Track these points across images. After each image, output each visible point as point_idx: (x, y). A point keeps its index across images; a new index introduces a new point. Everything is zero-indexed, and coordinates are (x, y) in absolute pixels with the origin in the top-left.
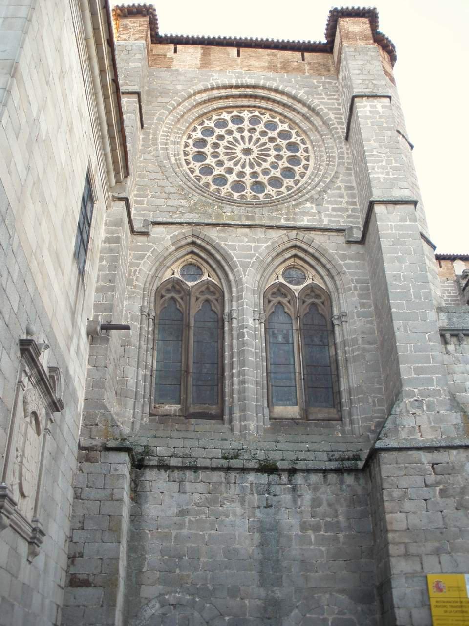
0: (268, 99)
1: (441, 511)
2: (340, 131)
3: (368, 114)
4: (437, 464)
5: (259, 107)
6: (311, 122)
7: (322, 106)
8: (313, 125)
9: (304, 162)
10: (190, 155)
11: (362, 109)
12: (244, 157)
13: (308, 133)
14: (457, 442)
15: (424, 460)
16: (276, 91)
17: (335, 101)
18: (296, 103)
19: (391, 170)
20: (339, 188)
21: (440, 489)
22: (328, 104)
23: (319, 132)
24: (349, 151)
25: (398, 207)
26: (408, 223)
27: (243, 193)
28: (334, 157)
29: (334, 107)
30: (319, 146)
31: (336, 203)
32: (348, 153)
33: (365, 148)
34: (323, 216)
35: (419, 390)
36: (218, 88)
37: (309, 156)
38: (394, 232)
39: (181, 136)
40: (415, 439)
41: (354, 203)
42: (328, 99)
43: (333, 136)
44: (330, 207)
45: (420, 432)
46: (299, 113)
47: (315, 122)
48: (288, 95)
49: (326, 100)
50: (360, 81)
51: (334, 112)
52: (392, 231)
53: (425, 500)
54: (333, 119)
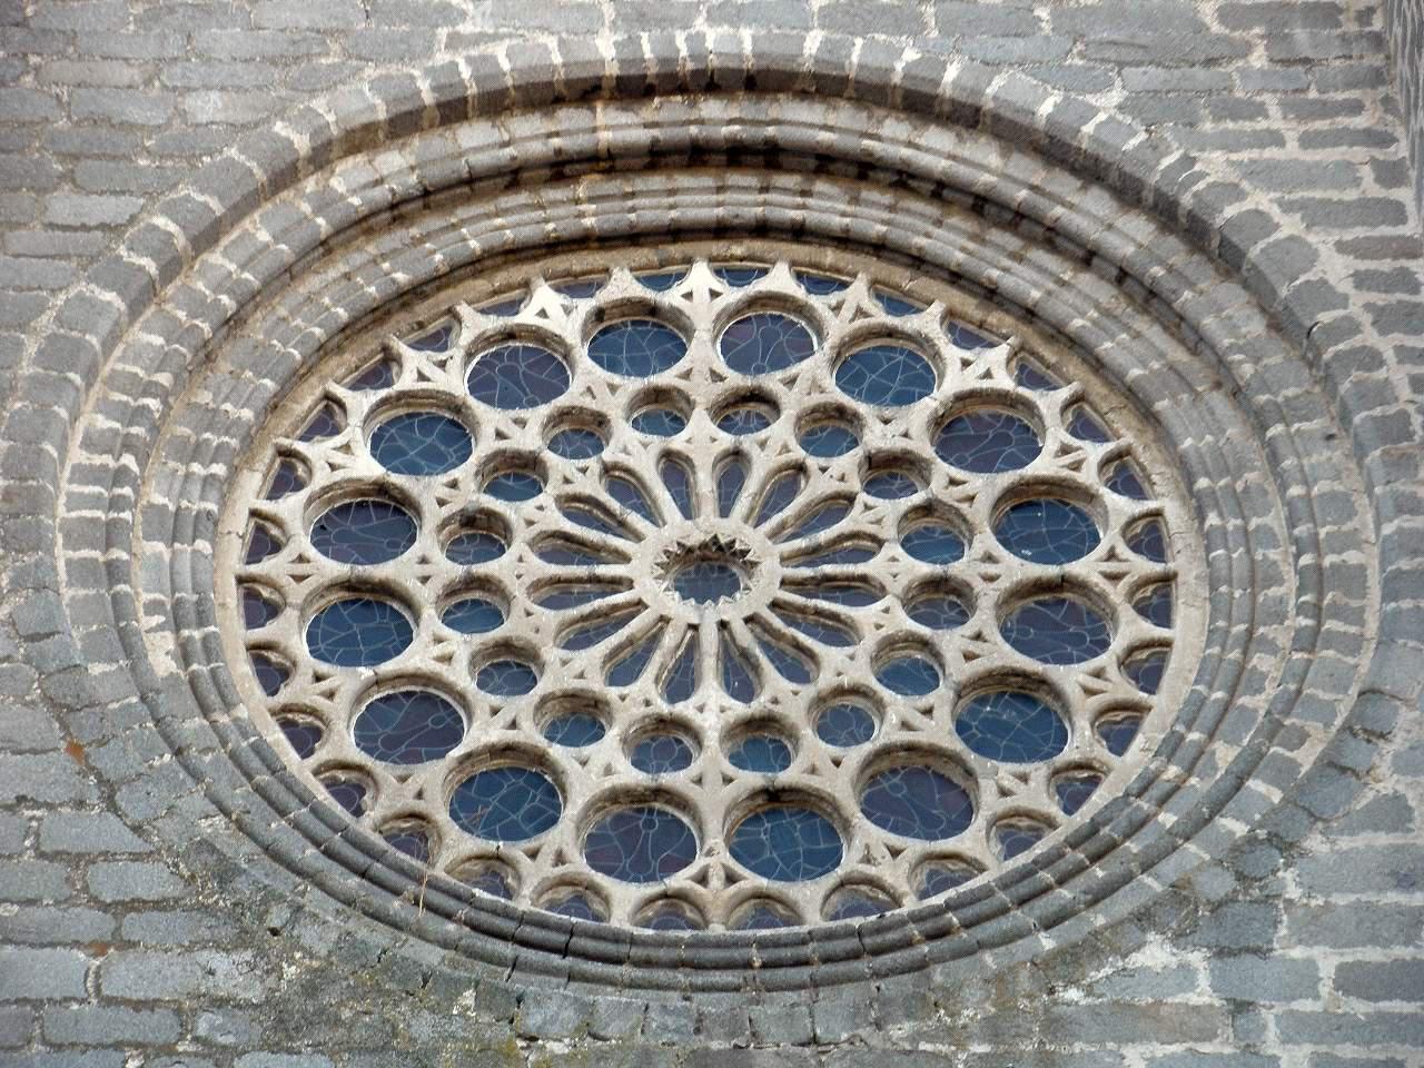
0: (862, 169)
5: (799, 233)
6: (1179, 325)
7: (1261, 199)
8: (1197, 342)
9: (1131, 628)
10: (290, 615)
12: (682, 610)
13: (1162, 405)
16: (920, 104)
17: (1359, 153)
18: (1064, 184)
22: (1311, 176)
23: (1237, 393)
27: (680, 880)
28: (1353, 579)
29: (1351, 195)
30: (1241, 503)
34: (1272, 1032)
36: (495, 104)
37: (1167, 579)
39: (219, 469)
42: (1307, 141)
43: (1345, 418)
44: (1327, 962)
46: (1088, 257)
47: (1209, 323)
48: (1011, 132)
49: (1292, 149)
51: (1348, 236)
54: (1345, 287)
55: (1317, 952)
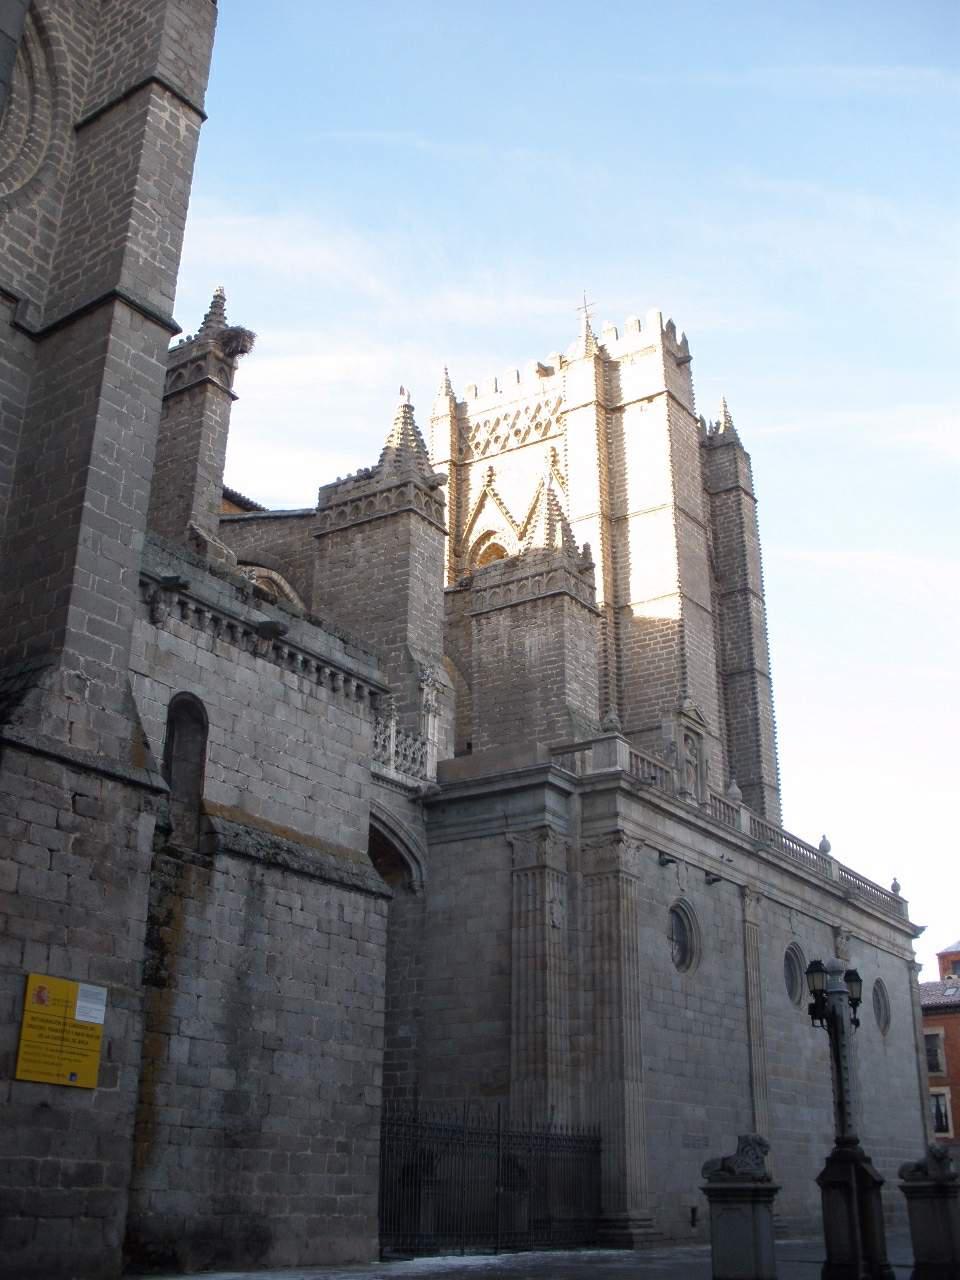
1: (69, 876)
2: (72, 105)
3: (163, 127)
4: (80, 795)
7: (61, 36)
11: (156, 110)
14: (119, 770)
15: (65, 783)
17: (84, 40)
19: (160, 252)
20: (33, 214)
21: (76, 839)
22: (73, 38)
24: (72, 154)
26: (154, 361)
28: (40, 146)
30: (21, 107)
31: (18, 239)
32: (68, 156)
33: (136, 188)
35: (86, 660)
40: (62, 742)
41: (45, 257)
45: (70, 733)
47: (34, 56)
49: (71, 28)
50: (171, 56)
51: (77, 61)
52: (126, 361)
53: (51, 850)
55: (7, 238)
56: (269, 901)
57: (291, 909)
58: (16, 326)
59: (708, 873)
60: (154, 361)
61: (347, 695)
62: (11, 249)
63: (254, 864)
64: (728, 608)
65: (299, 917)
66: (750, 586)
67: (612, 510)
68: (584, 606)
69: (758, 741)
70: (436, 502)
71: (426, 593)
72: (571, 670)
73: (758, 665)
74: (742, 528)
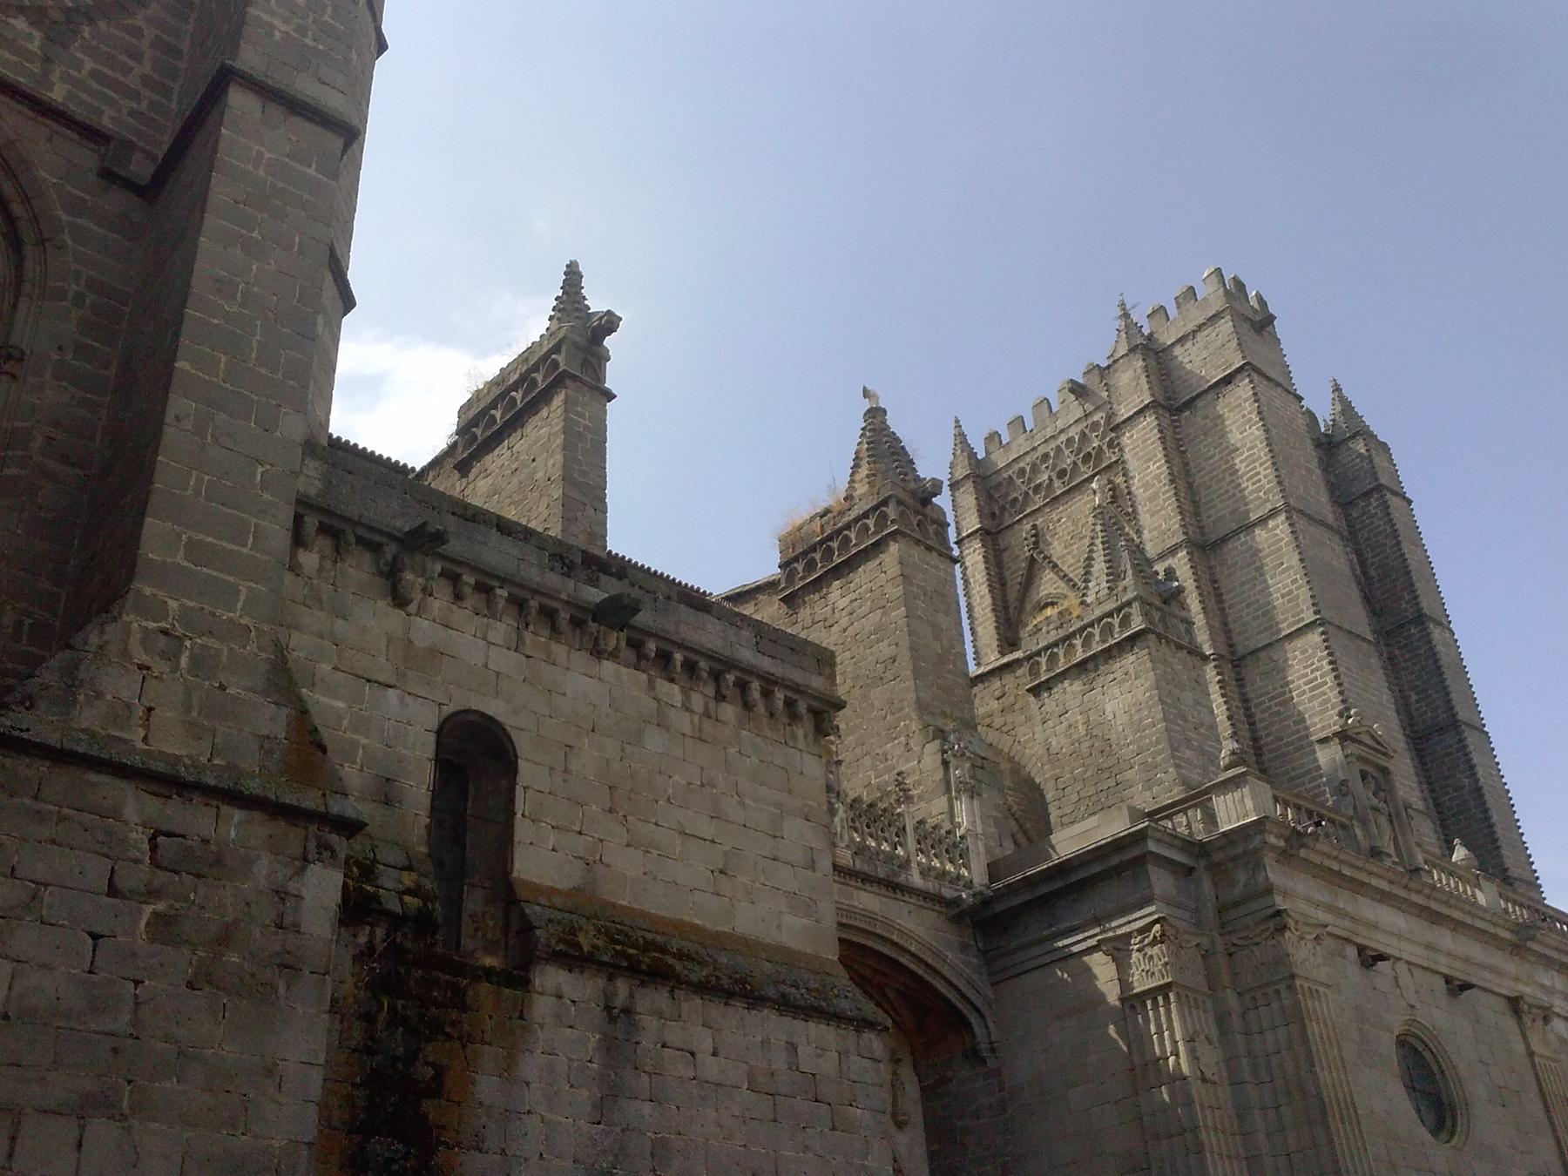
1: (137, 983)
4: (169, 835)
14: (253, 786)
15: (131, 812)
20: (137, 33)
21: (156, 914)
25: (297, 121)
26: (312, 171)
34: (57, 74)
35: (183, 606)
38: (261, 173)
40: (125, 741)
44: (89, 64)
45: (147, 727)
53: (95, 937)
56: (647, 1042)
57: (693, 1054)
58: (107, 174)
59: (1448, 980)
60: (312, 171)
61: (772, 715)
62: (94, 74)
63: (611, 978)
64: (1399, 648)
65: (711, 1068)
66: (1426, 611)
67: (1203, 534)
68: (1179, 647)
69: (1488, 819)
70: (933, 522)
71: (936, 638)
72: (1177, 732)
73: (1463, 714)
74: (1396, 537)
